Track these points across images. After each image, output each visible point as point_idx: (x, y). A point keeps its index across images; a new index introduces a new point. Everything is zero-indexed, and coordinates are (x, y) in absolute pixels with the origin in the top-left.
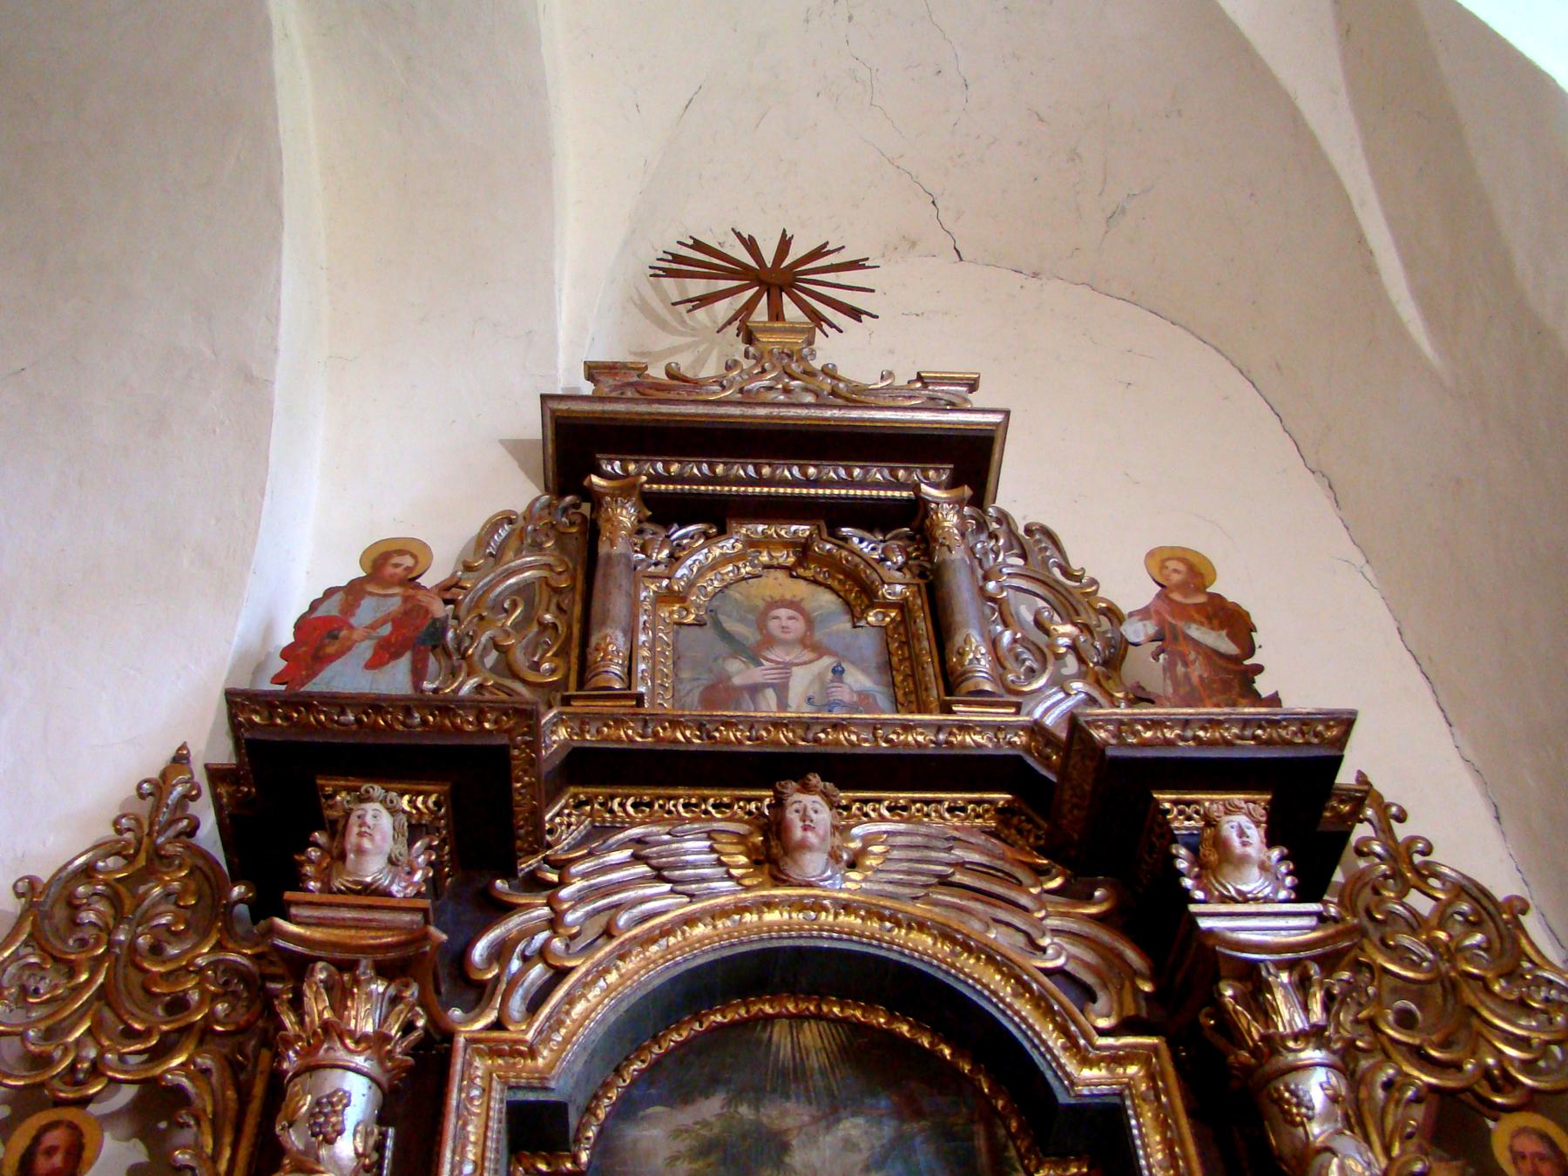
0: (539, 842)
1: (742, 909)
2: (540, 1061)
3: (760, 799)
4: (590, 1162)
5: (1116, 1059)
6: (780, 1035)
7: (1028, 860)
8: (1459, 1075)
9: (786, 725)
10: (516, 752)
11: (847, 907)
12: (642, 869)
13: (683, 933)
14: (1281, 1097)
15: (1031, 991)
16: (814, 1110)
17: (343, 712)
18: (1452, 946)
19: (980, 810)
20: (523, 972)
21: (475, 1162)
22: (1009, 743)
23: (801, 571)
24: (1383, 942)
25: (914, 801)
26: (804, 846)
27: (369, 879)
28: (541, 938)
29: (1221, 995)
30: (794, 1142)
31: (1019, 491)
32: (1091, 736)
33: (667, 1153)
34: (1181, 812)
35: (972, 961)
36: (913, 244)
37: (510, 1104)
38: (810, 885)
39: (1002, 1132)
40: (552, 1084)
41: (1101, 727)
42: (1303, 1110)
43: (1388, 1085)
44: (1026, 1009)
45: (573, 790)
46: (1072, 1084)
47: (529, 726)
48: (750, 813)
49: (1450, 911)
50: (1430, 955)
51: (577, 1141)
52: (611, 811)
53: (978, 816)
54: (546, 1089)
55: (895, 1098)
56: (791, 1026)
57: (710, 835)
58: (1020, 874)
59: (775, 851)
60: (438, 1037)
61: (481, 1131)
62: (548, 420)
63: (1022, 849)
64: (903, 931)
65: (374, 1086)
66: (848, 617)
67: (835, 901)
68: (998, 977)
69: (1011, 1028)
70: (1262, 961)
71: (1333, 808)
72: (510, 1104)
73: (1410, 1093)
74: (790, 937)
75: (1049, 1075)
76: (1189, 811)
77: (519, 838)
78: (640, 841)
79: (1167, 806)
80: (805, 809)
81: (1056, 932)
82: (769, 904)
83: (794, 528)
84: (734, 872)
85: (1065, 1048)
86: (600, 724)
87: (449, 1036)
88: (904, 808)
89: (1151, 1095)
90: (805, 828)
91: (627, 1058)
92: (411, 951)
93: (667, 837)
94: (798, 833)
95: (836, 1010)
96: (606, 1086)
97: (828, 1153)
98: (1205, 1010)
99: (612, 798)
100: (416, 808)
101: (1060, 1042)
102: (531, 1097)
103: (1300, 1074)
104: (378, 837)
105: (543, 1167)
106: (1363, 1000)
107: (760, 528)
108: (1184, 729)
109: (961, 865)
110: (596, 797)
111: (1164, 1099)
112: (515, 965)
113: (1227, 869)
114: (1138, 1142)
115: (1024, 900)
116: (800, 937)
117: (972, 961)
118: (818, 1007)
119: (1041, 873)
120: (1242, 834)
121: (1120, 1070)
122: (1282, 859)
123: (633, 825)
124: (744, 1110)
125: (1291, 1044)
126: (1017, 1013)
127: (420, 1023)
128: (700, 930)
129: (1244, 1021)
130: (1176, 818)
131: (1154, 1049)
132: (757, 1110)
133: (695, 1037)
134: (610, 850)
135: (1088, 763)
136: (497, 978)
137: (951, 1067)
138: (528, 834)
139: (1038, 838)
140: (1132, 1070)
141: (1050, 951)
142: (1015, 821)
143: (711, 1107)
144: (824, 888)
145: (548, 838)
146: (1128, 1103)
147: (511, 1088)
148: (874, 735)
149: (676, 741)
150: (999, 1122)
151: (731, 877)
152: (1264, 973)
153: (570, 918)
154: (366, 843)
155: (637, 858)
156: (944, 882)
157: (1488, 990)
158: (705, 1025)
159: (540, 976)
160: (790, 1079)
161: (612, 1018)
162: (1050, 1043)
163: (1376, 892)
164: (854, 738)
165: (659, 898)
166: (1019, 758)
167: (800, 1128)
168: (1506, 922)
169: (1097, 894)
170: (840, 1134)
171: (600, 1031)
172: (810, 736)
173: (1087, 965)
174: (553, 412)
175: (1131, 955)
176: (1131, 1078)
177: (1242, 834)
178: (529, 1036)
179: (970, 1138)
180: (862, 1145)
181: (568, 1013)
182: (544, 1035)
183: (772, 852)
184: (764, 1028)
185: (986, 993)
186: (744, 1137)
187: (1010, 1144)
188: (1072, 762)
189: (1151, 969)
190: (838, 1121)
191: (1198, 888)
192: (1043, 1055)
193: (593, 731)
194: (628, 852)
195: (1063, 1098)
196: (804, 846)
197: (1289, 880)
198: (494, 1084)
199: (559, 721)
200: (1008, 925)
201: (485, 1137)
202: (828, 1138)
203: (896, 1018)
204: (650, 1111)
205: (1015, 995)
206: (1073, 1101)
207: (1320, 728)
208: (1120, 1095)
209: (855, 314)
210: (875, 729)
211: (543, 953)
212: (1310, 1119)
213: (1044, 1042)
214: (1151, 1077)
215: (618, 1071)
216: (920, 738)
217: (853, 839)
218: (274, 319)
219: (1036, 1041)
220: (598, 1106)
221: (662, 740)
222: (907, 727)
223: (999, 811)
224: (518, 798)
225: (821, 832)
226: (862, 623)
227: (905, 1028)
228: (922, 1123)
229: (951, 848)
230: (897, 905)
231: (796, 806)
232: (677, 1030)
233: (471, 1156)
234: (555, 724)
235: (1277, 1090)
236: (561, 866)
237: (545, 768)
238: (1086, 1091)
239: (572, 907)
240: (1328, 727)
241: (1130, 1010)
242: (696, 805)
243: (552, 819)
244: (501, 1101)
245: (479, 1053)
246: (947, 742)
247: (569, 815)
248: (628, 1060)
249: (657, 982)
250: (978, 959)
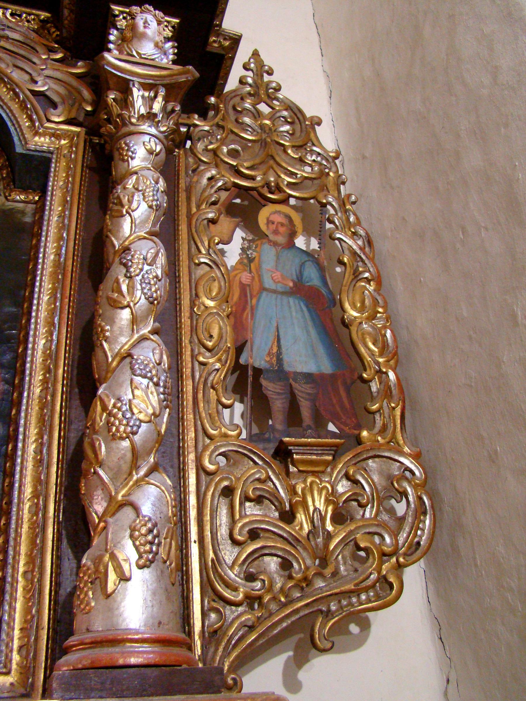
7: (46, 43)
8: (254, 182)
15: (19, 97)
18: (273, 129)
24: (237, 121)
29: (107, 97)
42: (130, 154)
43: (210, 179)
46: (26, 143)
49: (278, 115)
50: (259, 131)
58: (38, 49)
63: (48, 40)
68: (5, 90)
70: (133, 81)
73: (220, 184)
75: (16, 139)
79: (117, 13)
85: (28, 127)
103: (135, 136)
106: (213, 141)
111: (73, 156)
113: (135, 41)
115: (35, 60)
119: (51, 50)
120: (146, 22)
122: (173, 47)
130: (121, 20)
131: (78, 134)
140: (63, 142)
141: (40, 83)
152: (131, 86)
157: (285, 152)
163: (242, 99)
168: (307, 125)
169: (79, 64)
173: (58, 93)
176: (62, 146)
177: (146, 22)
195: (19, 149)
197: (171, 57)
200: (22, 69)
205: (12, 99)
206: (24, 152)
212: (132, 158)
223: (42, 21)
235: (120, 144)
241: (73, 115)
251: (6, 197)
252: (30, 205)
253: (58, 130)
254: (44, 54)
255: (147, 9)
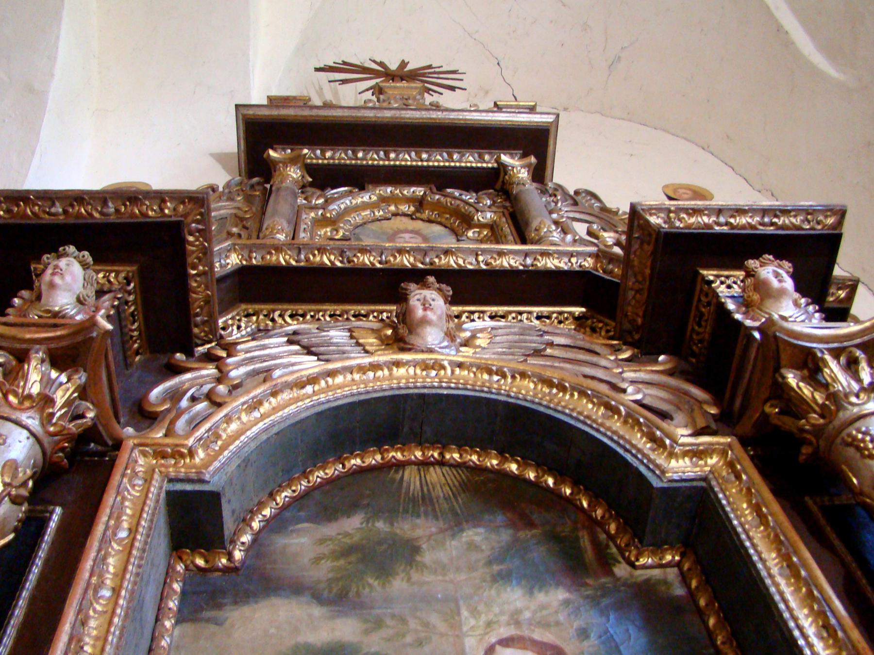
0: (214, 334)
1: (375, 367)
2: (197, 460)
3: (391, 312)
4: (243, 562)
5: (697, 454)
6: (410, 475)
9: (408, 252)
10: (191, 239)
11: (460, 365)
12: (296, 348)
13: (327, 382)
14: (855, 438)
16: (441, 524)
17: (53, 205)
19: (561, 318)
20: (189, 408)
21: (130, 530)
22: (580, 266)
23: (418, 215)
25: (510, 312)
26: (424, 321)
27: (57, 309)
28: (206, 388)
30: (424, 546)
31: (568, 170)
32: (648, 222)
33: (312, 555)
34: (722, 283)
35: (567, 397)
36: (487, 93)
37: (168, 493)
38: (431, 351)
39: (603, 537)
40: (207, 477)
41: (655, 214)
44: (616, 424)
45: (243, 306)
46: (663, 472)
47: (201, 214)
48: (382, 320)
51: (233, 542)
52: (273, 320)
53: (560, 322)
54: (202, 481)
55: (509, 515)
56: (419, 470)
57: (350, 330)
58: (598, 349)
59: (401, 331)
60: (110, 443)
61: (139, 508)
62: (241, 122)
64: (509, 380)
65: (32, 439)
66: (454, 236)
67: (451, 363)
68: (590, 406)
69: (605, 440)
71: (833, 294)
72: (168, 493)
74: (416, 387)
75: (642, 469)
76: (729, 282)
77: (196, 326)
78: (295, 333)
79: (711, 278)
80: (425, 297)
81: (633, 382)
82: (398, 364)
83: (412, 189)
84: (367, 348)
85: (653, 450)
86: (264, 252)
87: (118, 445)
88: (503, 317)
89: (732, 477)
90: (425, 309)
91: (280, 486)
92: (80, 338)
93: (317, 331)
94: (420, 312)
95: (456, 456)
96: (261, 505)
97: (454, 553)
98: (768, 404)
99: (274, 311)
100: (109, 281)
101: (649, 445)
102: (189, 487)
103: (868, 419)
104: (68, 278)
105: (200, 562)
107: (389, 189)
108: (718, 217)
109: (551, 344)
110: (262, 310)
111: (744, 477)
112: (184, 403)
114: (728, 509)
115: (603, 363)
116: (424, 387)
117: (567, 397)
118: (441, 454)
121: (701, 462)
123: (289, 325)
124: (380, 525)
125: (853, 399)
126: (609, 429)
127: (90, 415)
128: (339, 379)
129: (806, 391)
130: (718, 287)
131: (730, 445)
132: (392, 524)
133: (338, 478)
134: (271, 337)
135: (646, 247)
136: (168, 411)
137: (555, 494)
138: (204, 323)
139: (608, 331)
140: (713, 460)
142: (589, 322)
143: (352, 525)
144: (442, 354)
145: (222, 332)
146: (714, 483)
147: (171, 480)
148: (476, 260)
149: (323, 263)
150: (599, 530)
151: (367, 352)
152: (819, 355)
153: (233, 374)
154: (57, 280)
155: (290, 342)
156: (537, 353)
158: (348, 466)
159: (205, 410)
160: (422, 504)
161: (264, 437)
162: (640, 446)
164: (461, 262)
165: (309, 365)
166: (589, 272)
167: (430, 537)
170: (464, 539)
171: (253, 445)
172: (428, 260)
173: (661, 399)
174: (244, 116)
175: (696, 392)
176: (712, 466)
178: (190, 442)
179: (577, 539)
180: (484, 547)
181: (225, 430)
182: (205, 442)
183: (401, 335)
184: (397, 472)
185: (582, 418)
186: (380, 543)
187: (611, 544)
188: (633, 249)
189: (714, 400)
190: (462, 530)
191: (747, 319)
192: (635, 456)
193: (259, 258)
194: (286, 339)
195: (656, 483)
196: (424, 321)
198: (156, 476)
199: (232, 249)
201: (142, 510)
202: (453, 543)
203: (506, 459)
204: (300, 526)
206: (665, 485)
207: (821, 218)
208: (705, 479)
209: (452, 88)
210: (477, 255)
211: (209, 397)
213: (634, 446)
214: (731, 465)
215: (272, 496)
216: (512, 262)
217: (465, 330)
218: (53, 58)
219: (628, 446)
220: (252, 519)
221: (312, 263)
222: (501, 254)
224: (195, 285)
225: (439, 312)
226: (464, 238)
227: (514, 467)
228: (534, 531)
229: (541, 336)
230: (500, 364)
231: (418, 297)
232: (323, 468)
233: (125, 525)
234: (229, 251)
236: (230, 348)
237: (217, 276)
238: (676, 477)
239: (237, 368)
240: (826, 217)
241: (701, 423)
242: (339, 316)
243: (226, 322)
244: (161, 488)
245: (144, 454)
246: (532, 265)
247: (239, 320)
248: (281, 488)
249: (303, 415)
250: (572, 395)
251: (632, 565)
252: (668, 570)
253: (699, 445)
254: (611, 354)
255: (770, 260)
